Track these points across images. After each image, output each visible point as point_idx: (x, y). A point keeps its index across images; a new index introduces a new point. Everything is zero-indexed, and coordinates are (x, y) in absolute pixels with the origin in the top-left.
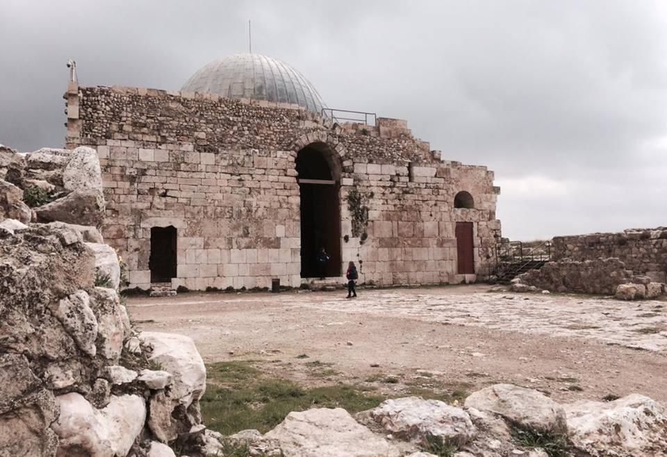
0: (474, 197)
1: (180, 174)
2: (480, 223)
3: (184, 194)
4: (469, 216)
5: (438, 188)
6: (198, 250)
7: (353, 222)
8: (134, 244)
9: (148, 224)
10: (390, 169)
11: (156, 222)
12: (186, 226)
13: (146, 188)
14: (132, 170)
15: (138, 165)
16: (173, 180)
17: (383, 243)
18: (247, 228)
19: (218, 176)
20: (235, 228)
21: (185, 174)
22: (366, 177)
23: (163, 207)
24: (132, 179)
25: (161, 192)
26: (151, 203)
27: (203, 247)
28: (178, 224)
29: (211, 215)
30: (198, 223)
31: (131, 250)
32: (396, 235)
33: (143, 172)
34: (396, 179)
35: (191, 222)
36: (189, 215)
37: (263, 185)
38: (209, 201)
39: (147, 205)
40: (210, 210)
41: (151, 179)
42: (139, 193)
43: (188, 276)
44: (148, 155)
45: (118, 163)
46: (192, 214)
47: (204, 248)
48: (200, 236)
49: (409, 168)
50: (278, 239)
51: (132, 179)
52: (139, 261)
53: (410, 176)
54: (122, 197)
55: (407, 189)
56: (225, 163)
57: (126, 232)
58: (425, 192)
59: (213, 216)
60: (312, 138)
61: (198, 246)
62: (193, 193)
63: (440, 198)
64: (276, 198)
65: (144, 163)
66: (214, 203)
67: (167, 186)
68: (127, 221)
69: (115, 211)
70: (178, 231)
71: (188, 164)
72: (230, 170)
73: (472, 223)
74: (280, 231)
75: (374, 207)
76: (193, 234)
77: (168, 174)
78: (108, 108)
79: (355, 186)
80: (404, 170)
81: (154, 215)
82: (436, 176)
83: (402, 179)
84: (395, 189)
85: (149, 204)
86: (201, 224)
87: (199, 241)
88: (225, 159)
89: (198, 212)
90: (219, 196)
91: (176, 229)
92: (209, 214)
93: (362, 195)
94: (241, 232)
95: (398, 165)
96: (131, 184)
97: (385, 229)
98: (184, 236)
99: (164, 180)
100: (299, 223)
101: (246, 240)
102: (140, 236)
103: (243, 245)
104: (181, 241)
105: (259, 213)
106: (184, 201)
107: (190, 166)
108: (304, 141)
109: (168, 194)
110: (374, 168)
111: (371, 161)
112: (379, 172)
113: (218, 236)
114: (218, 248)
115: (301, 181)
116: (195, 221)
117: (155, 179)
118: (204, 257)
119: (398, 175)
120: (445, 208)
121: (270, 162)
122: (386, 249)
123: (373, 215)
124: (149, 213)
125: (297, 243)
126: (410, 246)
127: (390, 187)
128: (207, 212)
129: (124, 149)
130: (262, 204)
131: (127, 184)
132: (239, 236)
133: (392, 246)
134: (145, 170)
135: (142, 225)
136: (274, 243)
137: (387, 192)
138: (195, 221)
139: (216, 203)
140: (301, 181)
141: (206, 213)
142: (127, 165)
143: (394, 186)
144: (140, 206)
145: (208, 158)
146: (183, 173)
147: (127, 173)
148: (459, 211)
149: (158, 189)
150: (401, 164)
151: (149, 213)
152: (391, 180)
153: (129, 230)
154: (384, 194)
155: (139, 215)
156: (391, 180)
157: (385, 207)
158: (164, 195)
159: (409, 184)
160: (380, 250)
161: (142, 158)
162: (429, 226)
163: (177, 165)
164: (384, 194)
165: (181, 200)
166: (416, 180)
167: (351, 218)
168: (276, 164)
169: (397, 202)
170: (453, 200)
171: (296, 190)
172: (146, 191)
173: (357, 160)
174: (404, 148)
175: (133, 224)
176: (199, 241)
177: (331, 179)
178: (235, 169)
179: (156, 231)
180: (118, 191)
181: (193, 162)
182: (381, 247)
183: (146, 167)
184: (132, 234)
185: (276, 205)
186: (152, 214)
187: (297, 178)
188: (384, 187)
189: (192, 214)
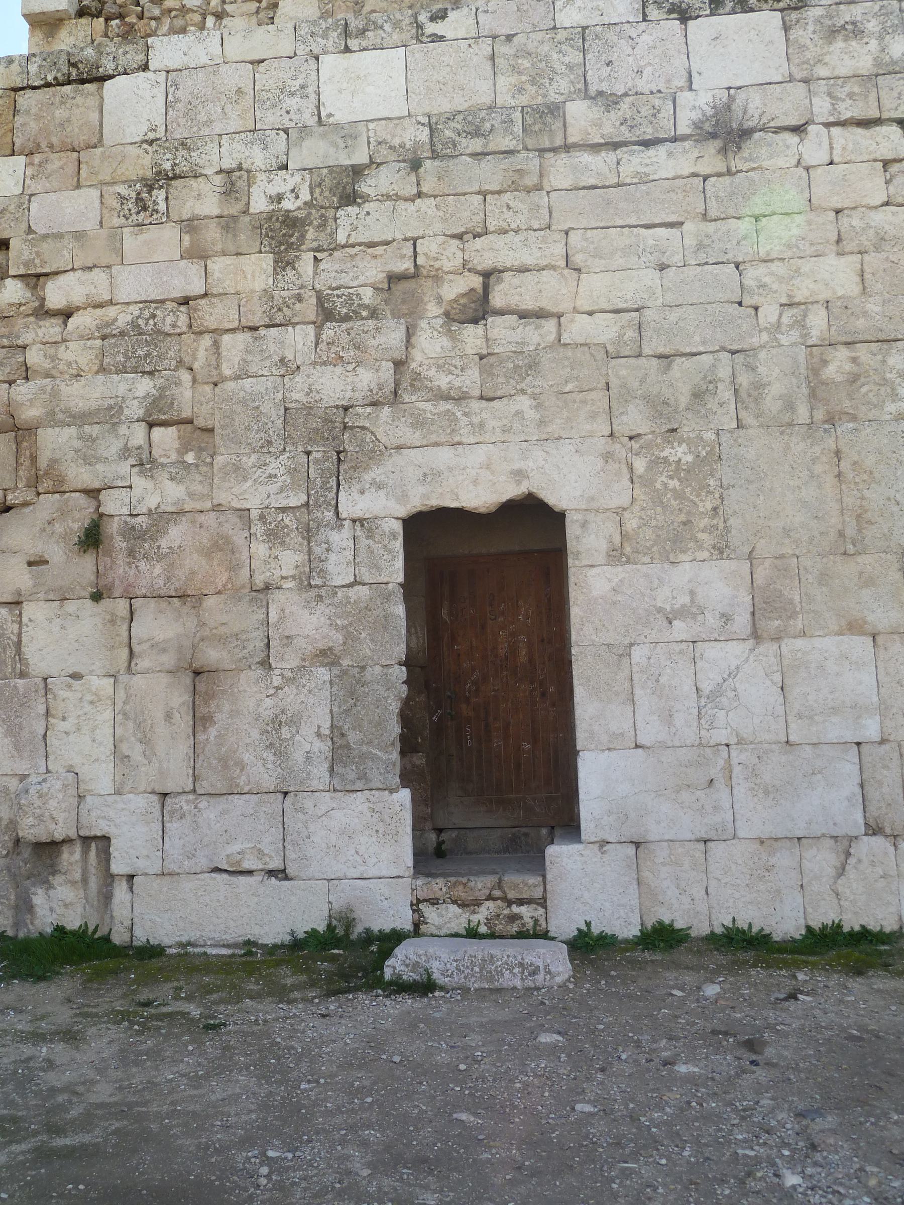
1: (561, 171)
3: (596, 287)
6: (712, 651)
9: (384, 499)
11: (430, 476)
12: (619, 494)
13: (364, 276)
14: (281, 183)
15: (316, 152)
16: (519, 210)
19: (814, 148)
21: (597, 165)
23: (471, 379)
24: (283, 235)
25: (455, 288)
26: (399, 364)
27: (742, 621)
28: (568, 479)
29: (790, 406)
30: (711, 458)
31: (286, 661)
33: (346, 187)
35: (657, 463)
36: (634, 418)
38: (769, 313)
39: (368, 379)
42: (327, 313)
43: (654, 832)
45: (214, 158)
46: (658, 406)
47: (756, 635)
48: (720, 551)
51: (283, 235)
52: (337, 733)
54: (234, 346)
57: (260, 549)
59: (803, 413)
61: (712, 620)
62: (651, 277)
65: (347, 134)
66: (801, 324)
67: (489, 252)
68: (264, 485)
69: (198, 433)
70: (572, 530)
71: (609, 101)
76: (674, 543)
77: (491, 174)
81: (416, 437)
85: (387, 371)
86: (725, 472)
87: (719, 585)
88: (855, 31)
89: (698, 395)
90: (837, 275)
91: (560, 517)
92: (771, 403)
96: (283, 263)
98: (617, 555)
99: (468, 212)
102: (339, 571)
104: (595, 587)
106: (604, 329)
107: (625, 105)
109: (497, 300)
113: (847, 545)
114: (854, 627)
116: (680, 453)
117: (410, 219)
118: (757, 692)
124: (386, 426)
128: (759, 386)
129: (240, 76)
131: (254, 271)
134: (357, 172)
135: (352, 503)
138: (680, 453)
139: (817, 321)
141: (747, 397)
142: (257, 158)
144: (332, 386)
146: (586, 158)
147: (259, 204)
149: (437, 277)
151: (386, 426)
153: (275, 536)
155: (334, 444)
158: (477, 309)
161: (339, 108)
165: (579, 328)
172: (367, 295)
175: (297, 499)
179: (430, 532)
180: (214, 314)
181: (643, 85)
183: (360, 157)
184: (290, 560)
186: (404, 433)
189: (658, 406)
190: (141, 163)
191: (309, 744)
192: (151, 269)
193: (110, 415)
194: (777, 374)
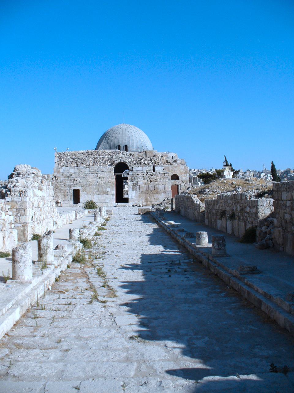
0: (179, 176)
2: (182, 185)
4: (177, 183)
5: (164, 173)
8: (69, 194)
9: (72, 189)
10: (146, 168)
15: (70, 173)
18: (98, 189)
20: (96, 189)
24: (68, 177)
31: (68, 195)
33: (71, 175)
34: (148, 171)
37: (103, 176)
40: (88, 184)
41: (73, 177)
44: (72, 170)
45: (65, 173)
46: (83, 185)
49: (154, 167)
50: (108, 192)
51: (68, 177)
55: (152, 175)
56: (92, 171)
58: (159, 175)
60: (119, 161)
63: (165, 177)
64: (107, 180)
65: (71, 173)
68: (67, 188)
72: (94, 173)
73: (178, 185)
74: (108, 189)
76: (84, 191)
78: (64, 158)
80: (152, 168)
82: (164, 170)
83: (150, 171)
90: (91, 180)
93: (135, 177)
94: (97, 190)
97: (144, 188)
98: (82, 191)
101: (98, 192)
102: (70, 192)
103: (97, 194)
104: (81, 193)
105: (102, 184)
106: (81, 182)
108: (116, 162)
119: (149, 170)
120: (167, 180)
121: (105, 170)
123: (140, 183)
124: (73, 186)
125: (114, 193)
130: (103, 182)
131: (67, 179)
132: (96, 191)
136: (107, 193)
137: (144, 176)
140: (116, 174)
143: (147, 174)
144: (70, 184)
145: (87, 170)
148: (173, 181)
151: (73, 186)
153: (68, 190)
158: (76, 181)
159: (153, 173)
161: (70, 171)
162: (161, 187)
163: (80, 173)
167: (131, 185)
168: (107, 170)
170: (170, 177)
171: (114, 177)
176: (85, 193)
177: (116, 175)
178: (96, 173)
179: (74, 190)
184: (69, 191)
185: (107, 182)
187: (115, 173)
188: (144, 174)
189: (83, 185)
190: (62, 173)
191: (69, 199)
192: (62, 179)
193: (61, 185)
194: (88, 184)
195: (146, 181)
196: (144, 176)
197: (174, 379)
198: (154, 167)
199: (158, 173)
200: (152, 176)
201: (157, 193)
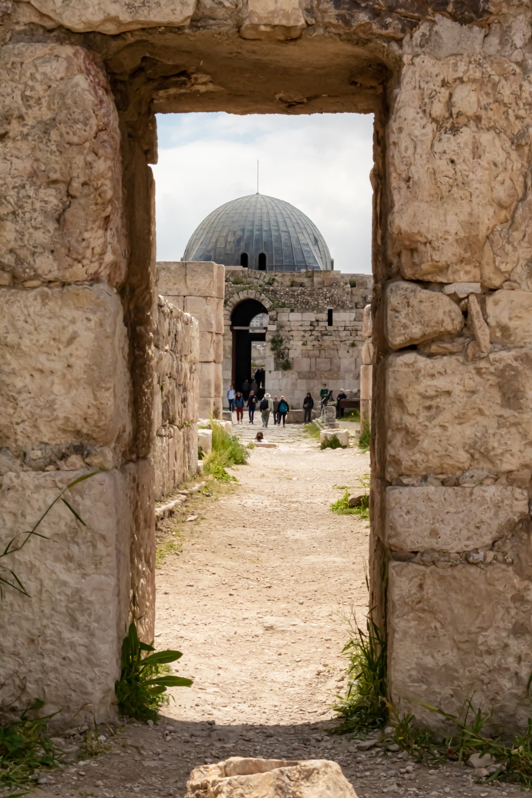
7: (275, 359)
10: (311, 316)
17: (301, 375)
22: (288, 323)
32: (313, 369)
34: (315, 324)
49: (330, 312)
53: (330, 321)
58: (343, 334)
60: (243, 296)
75: (295, 347)
79: (278, 331)
80: (324, 316)
82: (355, 320)
83: (321, 324)
84: (314, 333)
95: (318, 313)
97: (304, 365)
100: (231, 360)
110: (295, 316)
111: (292, 311)
112: (300, 319)
115: (236, 328)
119: (317, 321)
122: (304, 381)
126: (326, 378)
127: (311, 331)
133: (310, 378)
140: (236, 328)
150: (320, 311)
152: (311, 325)
154: (304, 336)
156: (311, 325)
157: (304, 348)
159: (329, 328)
160: (299, 381)
164: (304, 336)
166: (334, 324)
167: (273, 356)
169: (316, 343)
173: (279, 310)
174: (332, 296)
182: (300, 378)
188: (305, 331)
195: (309, 347)
196: (307, 335)
197: (365, 570)
198: (330, 312)
199: (340, 329)
200: (326, 335)
201: (338, 378)
